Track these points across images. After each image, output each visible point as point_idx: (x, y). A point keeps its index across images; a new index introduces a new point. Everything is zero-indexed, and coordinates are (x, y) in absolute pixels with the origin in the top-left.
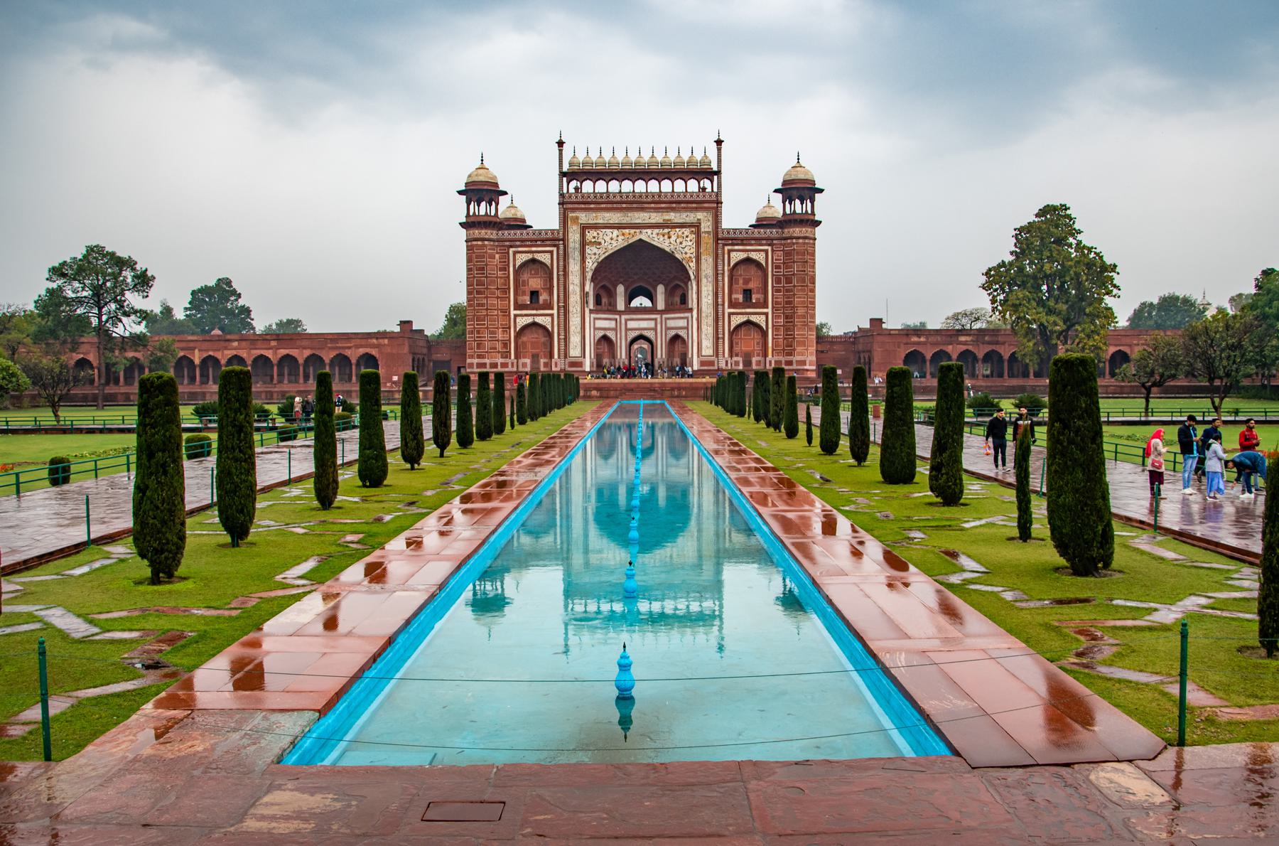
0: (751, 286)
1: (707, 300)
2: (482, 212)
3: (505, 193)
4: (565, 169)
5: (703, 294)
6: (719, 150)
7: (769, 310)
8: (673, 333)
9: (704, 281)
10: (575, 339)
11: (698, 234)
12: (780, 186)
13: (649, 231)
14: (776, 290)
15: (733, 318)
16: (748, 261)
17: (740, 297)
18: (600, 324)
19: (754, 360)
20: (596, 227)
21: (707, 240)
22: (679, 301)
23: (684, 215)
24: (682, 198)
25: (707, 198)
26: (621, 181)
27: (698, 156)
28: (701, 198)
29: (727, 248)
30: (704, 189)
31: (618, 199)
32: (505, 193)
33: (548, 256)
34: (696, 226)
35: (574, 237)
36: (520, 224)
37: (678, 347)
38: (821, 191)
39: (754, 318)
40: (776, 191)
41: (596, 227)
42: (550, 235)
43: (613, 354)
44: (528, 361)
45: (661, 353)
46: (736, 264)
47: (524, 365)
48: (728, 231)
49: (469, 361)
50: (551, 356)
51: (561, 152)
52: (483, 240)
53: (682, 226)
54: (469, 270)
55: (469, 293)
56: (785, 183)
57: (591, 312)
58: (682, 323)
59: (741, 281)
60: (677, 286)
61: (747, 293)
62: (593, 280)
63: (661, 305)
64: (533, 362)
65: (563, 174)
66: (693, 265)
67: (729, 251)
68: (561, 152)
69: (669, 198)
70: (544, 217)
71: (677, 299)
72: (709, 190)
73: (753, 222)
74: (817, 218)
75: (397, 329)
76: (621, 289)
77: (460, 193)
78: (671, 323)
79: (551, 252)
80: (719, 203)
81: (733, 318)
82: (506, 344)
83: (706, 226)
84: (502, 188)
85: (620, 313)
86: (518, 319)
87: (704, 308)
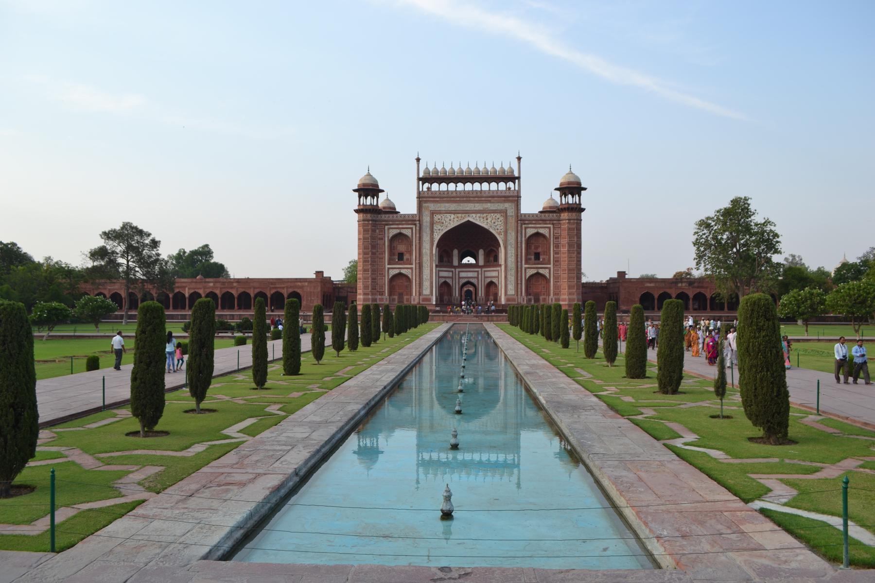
0: (539, 250)
1: (512, 260)
2: (368, 203)
3: (383, 191)
4: (421, 176)
5: (507, 254)
6: (519, 163)
7: (551, 266)
8: (489, 280)
9: (509, 247)
10: (426, 284)
11: (506, 217)
12: (558, 186)
14: (556, 253)
15: (528, 270)
16: (537, 235)
17: (533, 257)
18: (442, 274)
19: (541, 298)
20: (440, 212)
21: (512, 221)
22: (492, 258)
23: (496, 205)
24: (495, 194)
25: (511, 194)
26: (456, 183)
27: (506, 168)
28: (507, 194)
30: (510, 188)
31: (454, 194)
32: (383, 191)
33: (410, 231)
34: (504, 212)
35: (426, 219)
36: (391, 210)
37: (492, 289)
38: (585, 189)
39: (541, 271)
40: (556, 189)
41: (440, 212)
42: (411, 218)
43: (450, 293)
44: (396, 297)
45: (481, 293)
47: (394, 300)
48: (525, 215)
49: (358, 297)
50: (411, 294)
52: (368, 221)
53: (494, 212)
54: (359, 239)
55: (359, 254)
57: (437, 266)
58: (495, 274)
60: (492, 251)
62: (438, 246)
63: (481, 263)
64: (399, 298)
65: (419, 179)
69: (487, 194)
70: (407, 206)
71: (492, 259)
72: (512, 189)
73: (541, 210)
75: (314, 276)
76: (456, 252)
77: (355, 191)
78: (488, 274)
79: (412, 228)
80: (519, 197)
81: (528, 270)
82: (383, 286)
84: (381, 188)
85: (455, 267)
86: (391, 271)
87: (509, 264)
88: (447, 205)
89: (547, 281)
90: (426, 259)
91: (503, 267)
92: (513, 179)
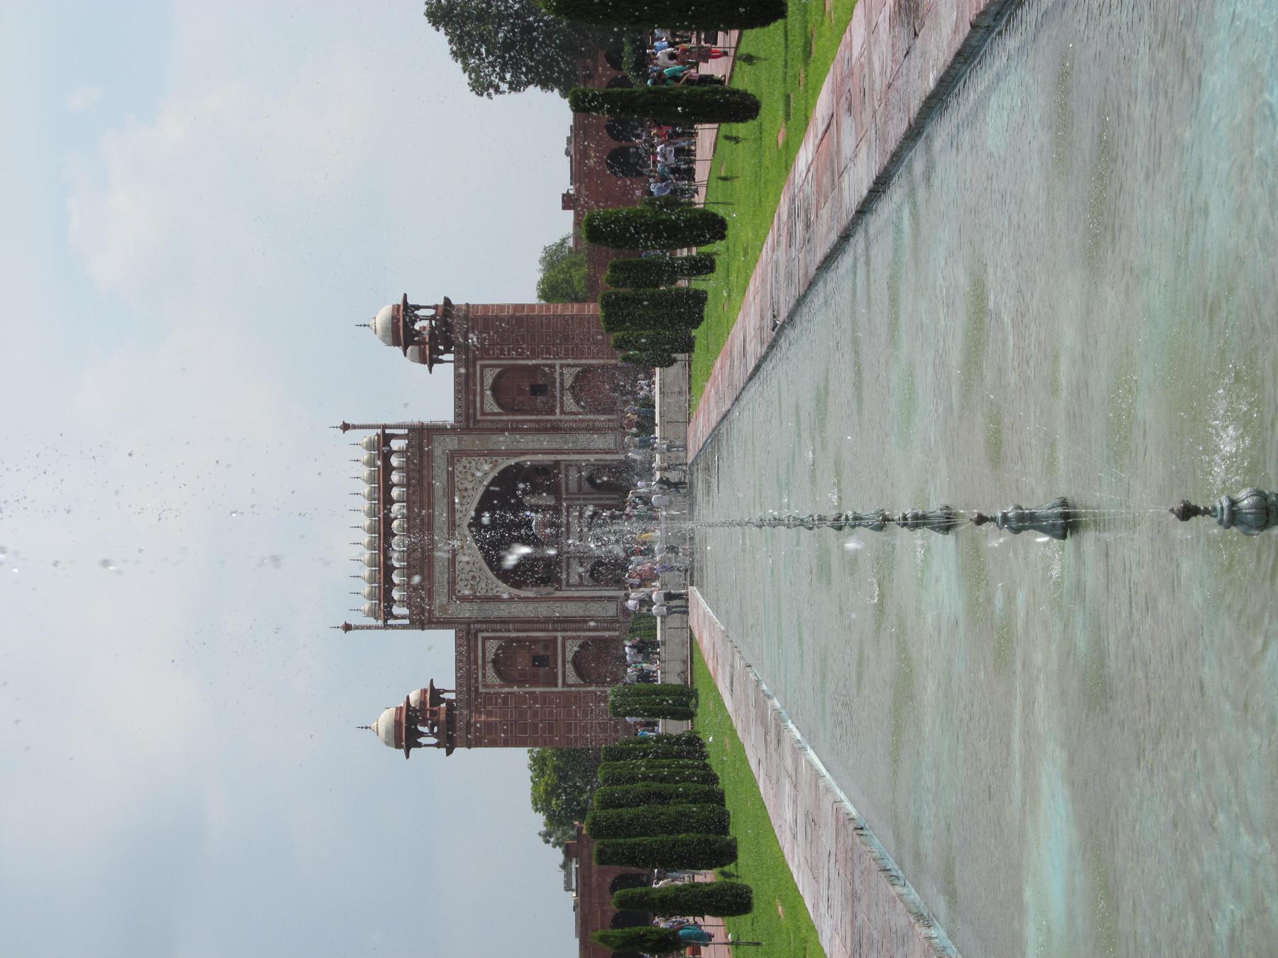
1: (545, 441)
5: (534, 448)
6: (355, 427)
8: (586, 486)
10: (595, 609)
13: (458, 515)
17: (540, 399)
20: (452, 582)
23: (437, 472)
29: (479, 417)
33: (488, 643)
34: (453, 457)
35: (467, 611)
41: (452, 582)
46: (500, 405)
48: (457, 415)
51: (357, 628)
53: (451, 475)
54: (506, 744)
56: (396, 342)
59: (521, 398)
61: (538, 390)
65: (386, 627)
66: (500, 460)
67: (483, 414)
68: (357, 628)
74: (441, 302)
77: (408, 757)
78: (573, 486)
83: (451, 443)
87: (554, 446)
88: (437, 569)
89: (587, 370)
90: (543, 610)
91: (559, 457)
92: (387, 439)
